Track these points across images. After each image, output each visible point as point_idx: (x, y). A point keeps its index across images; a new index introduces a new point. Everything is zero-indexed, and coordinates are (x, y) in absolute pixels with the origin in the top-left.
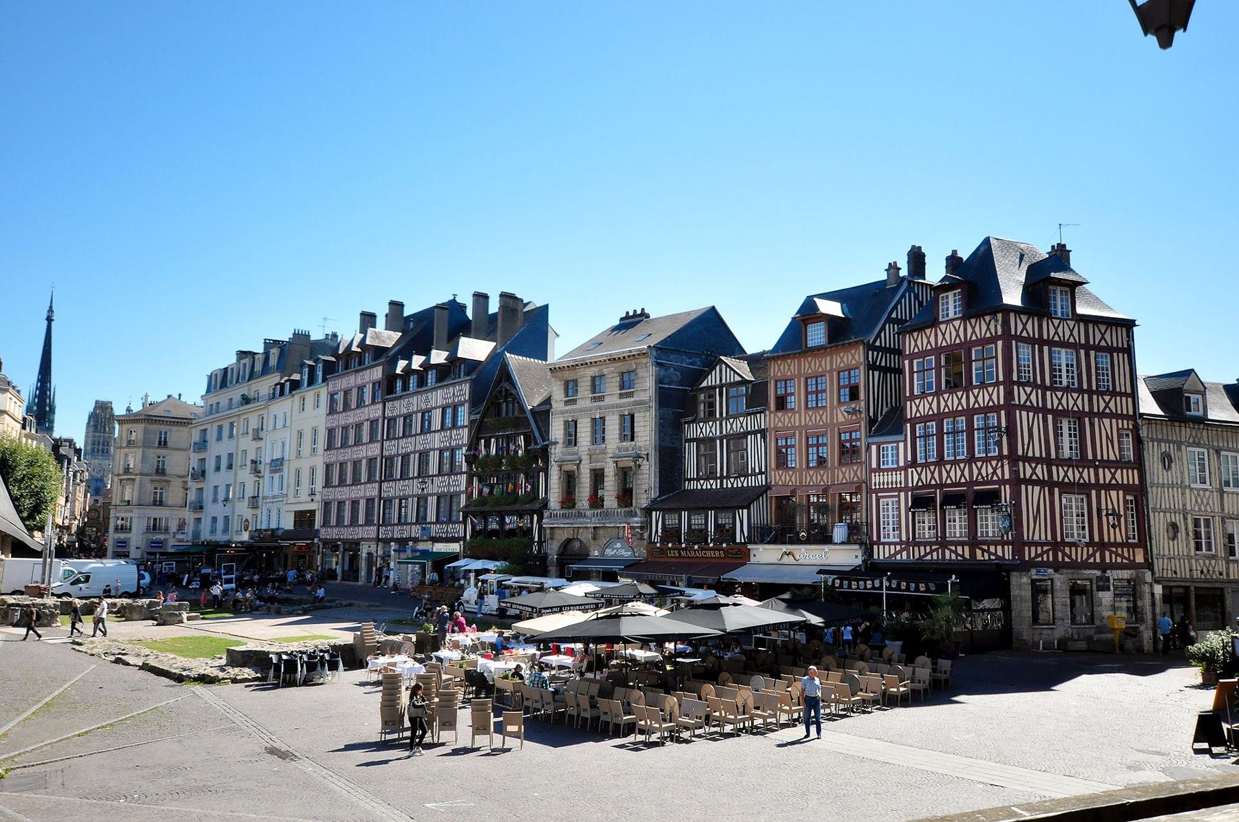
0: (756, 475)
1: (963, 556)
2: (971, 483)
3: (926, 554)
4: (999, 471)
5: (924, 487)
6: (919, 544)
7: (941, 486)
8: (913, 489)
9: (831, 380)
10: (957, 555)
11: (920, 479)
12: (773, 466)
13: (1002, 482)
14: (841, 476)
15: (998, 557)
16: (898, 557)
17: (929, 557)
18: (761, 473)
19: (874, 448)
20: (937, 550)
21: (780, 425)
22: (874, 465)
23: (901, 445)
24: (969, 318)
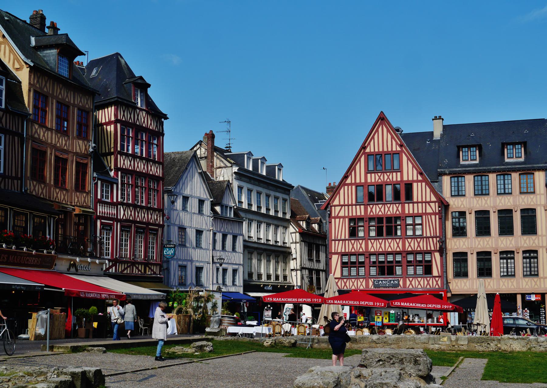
0: (13, 178)
1: (141, 271)
2: (148, 224)
3: (124, 270)
4: (158, 219)
5: (127, 220)
6: (122, 262)
7: (134, 222)
8: (120, 221)
9: (73, 113)
10: (139, 270)
11: (124, 214)
12: (29, 175)
13: (159, 225)
14: (76, 200)
15: (155, 273)
16: (111, 270)
17: (125, 272)
18: (16, 178)
19: (99, 182)
20: (129, 266)
21: (36, 136)
22: (99, 197)
23: (115, 186)
24: (150, 114)
